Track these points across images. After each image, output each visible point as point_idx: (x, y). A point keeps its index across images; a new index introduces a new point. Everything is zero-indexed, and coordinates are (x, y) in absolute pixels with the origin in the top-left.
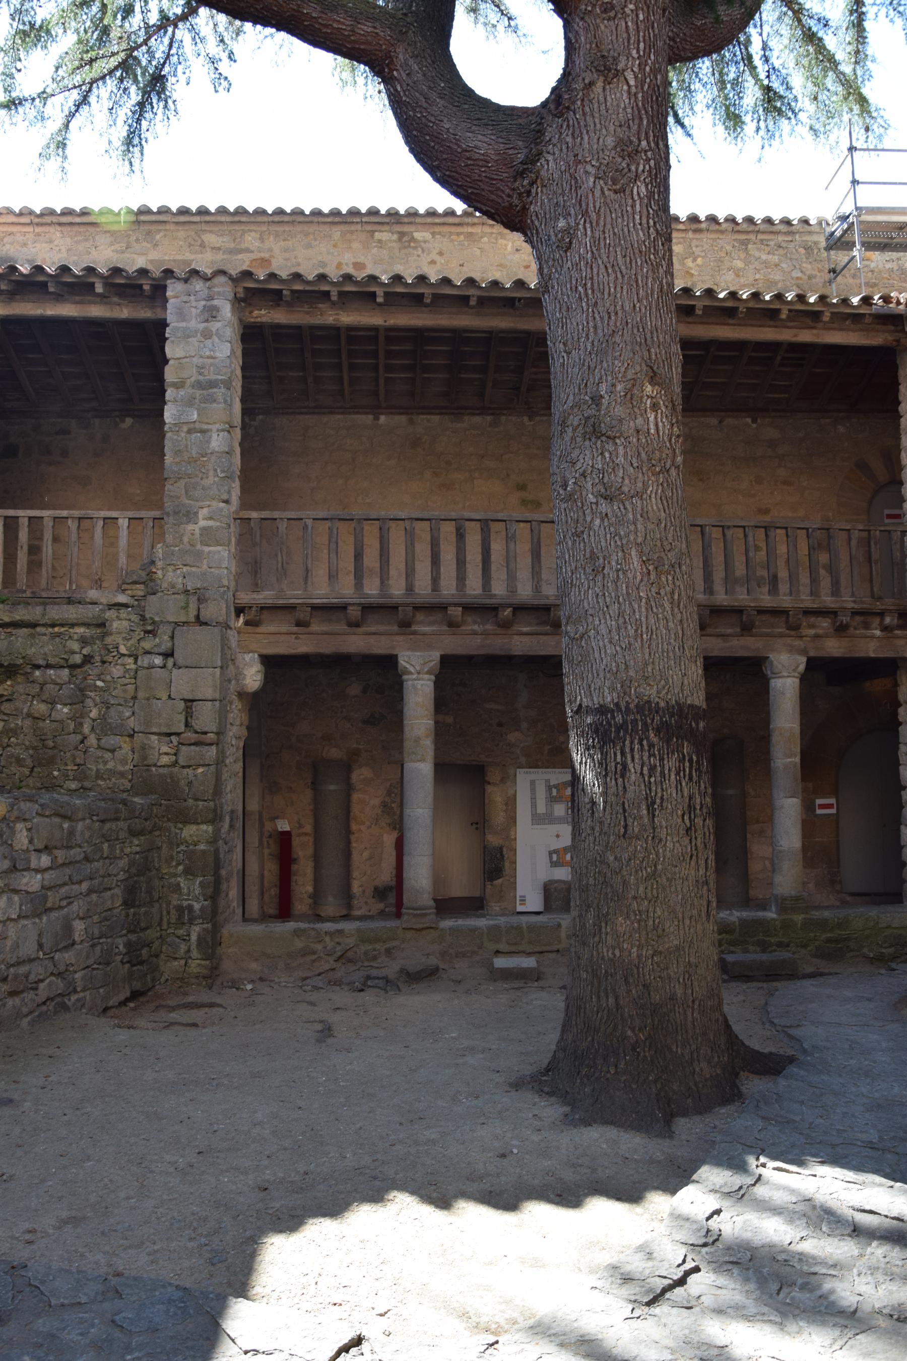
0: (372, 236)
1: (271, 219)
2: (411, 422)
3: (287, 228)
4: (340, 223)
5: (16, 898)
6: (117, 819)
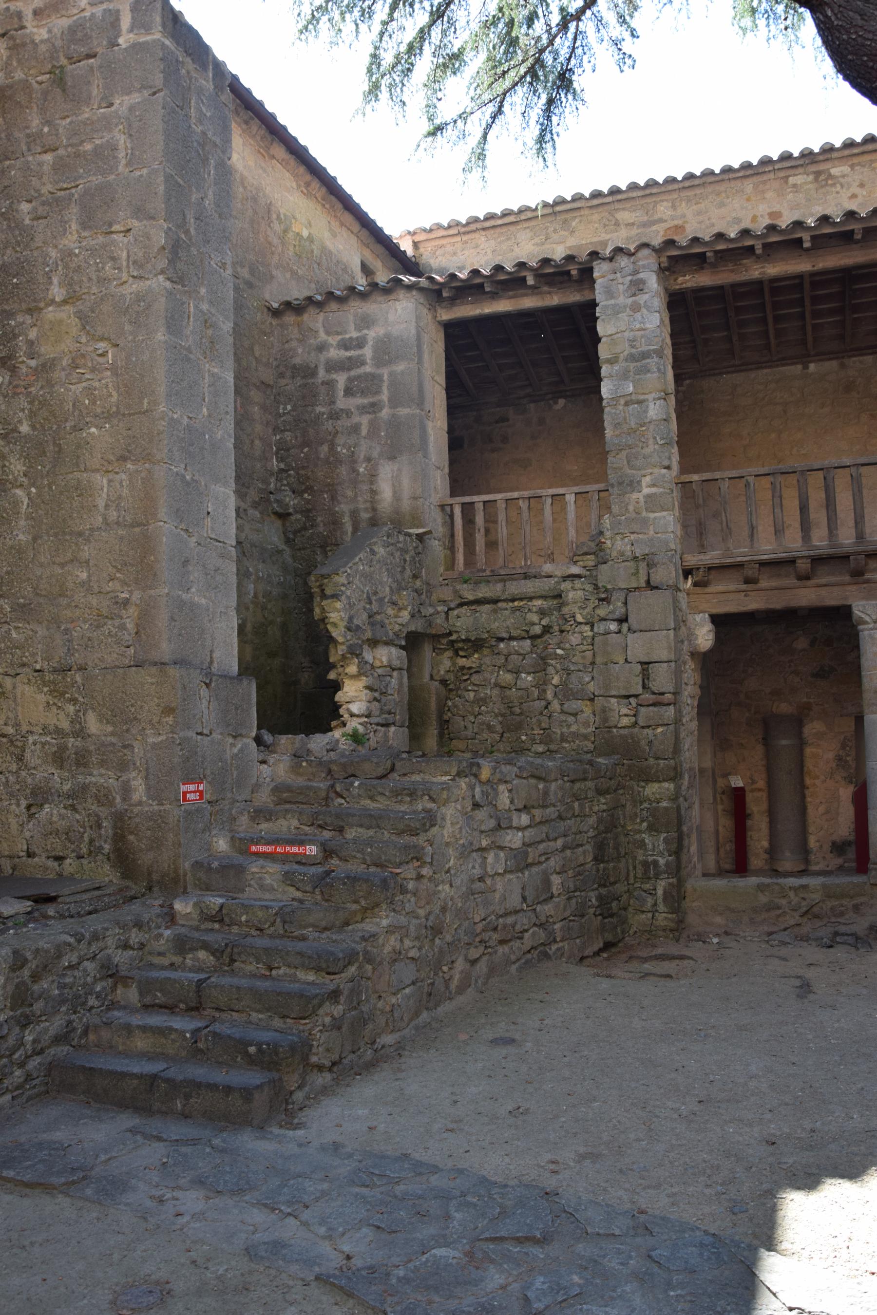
0: (786, 182)
1: (681, 185)
3: (698, 191)
4: (752, 175)
5: (502, 854)
6: (585, 779)
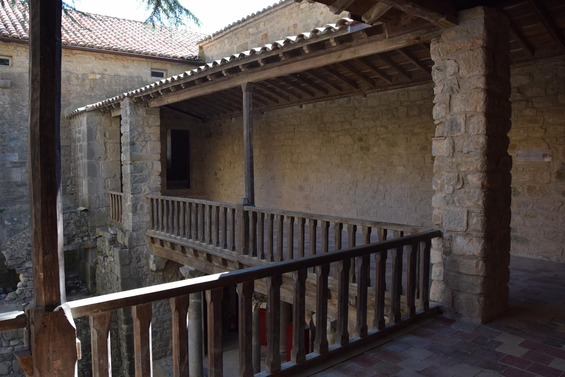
0: (299, 8)
2: (314, 106)
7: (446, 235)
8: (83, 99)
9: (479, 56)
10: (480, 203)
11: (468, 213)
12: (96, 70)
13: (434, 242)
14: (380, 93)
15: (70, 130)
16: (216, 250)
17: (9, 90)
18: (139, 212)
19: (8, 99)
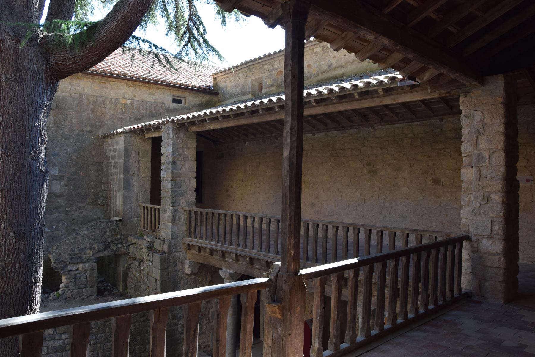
0: (313, 51)
2: (326, 135)
7: (474, 238)
8: (115, 121)
9: (500, 110)
10: (501, 214)
11: (492, 222)
12: (126, 96)
13: (465, 244)
14: (387, 126)
15: (103, 148)
16: (260, 255)
17: (54, 112)
18: (177, 222)
19: (53, 119)
